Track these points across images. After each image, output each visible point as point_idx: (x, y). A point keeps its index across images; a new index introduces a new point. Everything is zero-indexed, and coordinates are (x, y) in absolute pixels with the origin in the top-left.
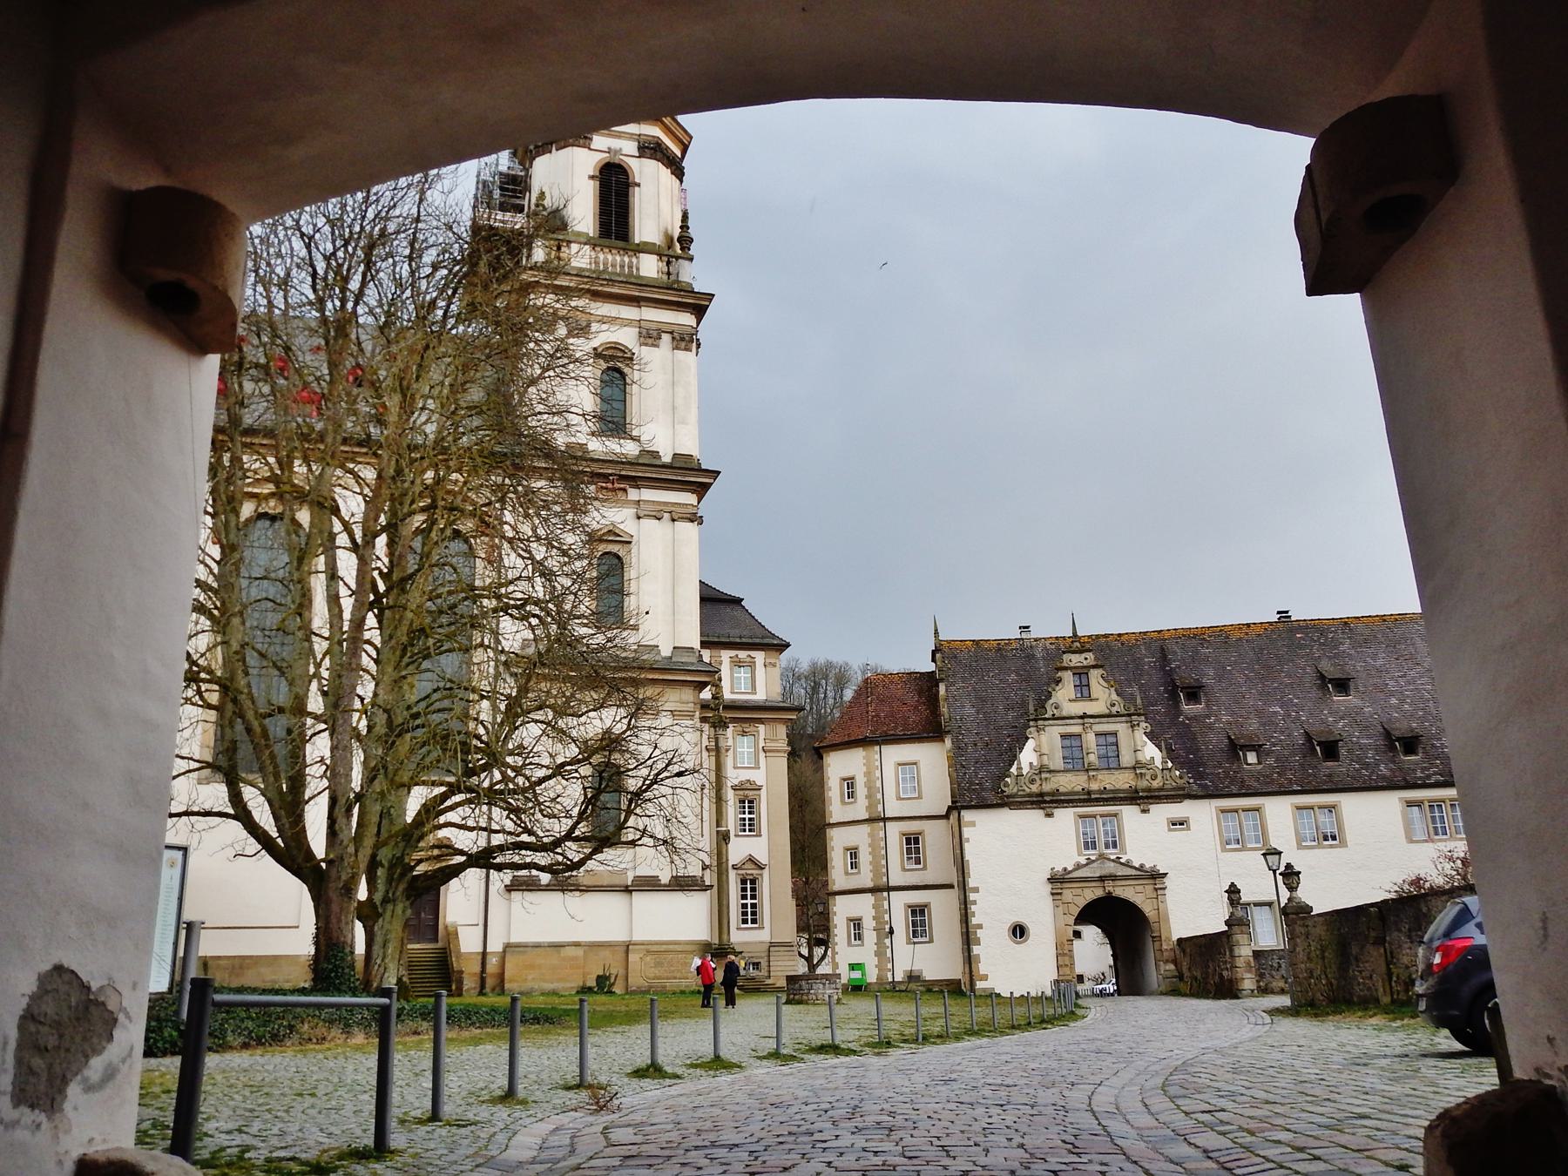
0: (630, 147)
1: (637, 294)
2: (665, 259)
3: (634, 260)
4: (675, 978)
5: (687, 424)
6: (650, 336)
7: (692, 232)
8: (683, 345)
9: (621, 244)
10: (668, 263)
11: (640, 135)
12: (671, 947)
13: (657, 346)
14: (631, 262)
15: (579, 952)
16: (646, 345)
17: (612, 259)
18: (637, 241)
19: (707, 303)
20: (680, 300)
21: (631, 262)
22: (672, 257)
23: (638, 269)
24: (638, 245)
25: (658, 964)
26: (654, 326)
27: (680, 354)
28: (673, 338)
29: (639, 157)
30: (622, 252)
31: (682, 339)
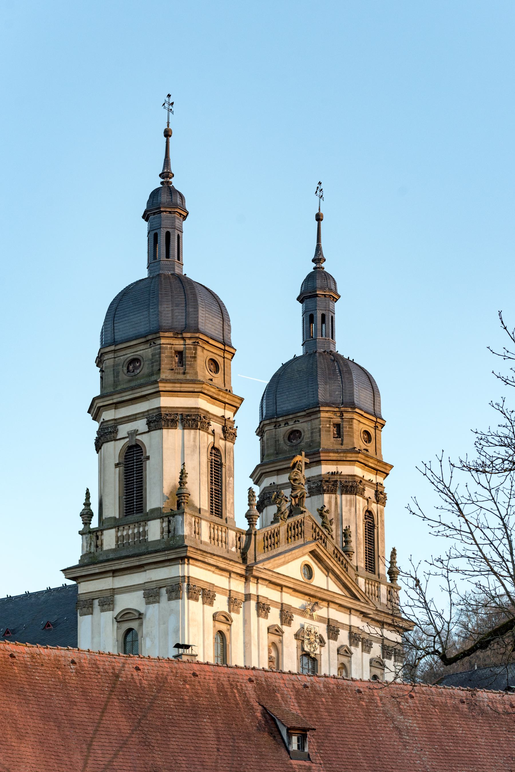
0: (141, 425)
2: (166, 519)
8: (174, 594)
11: (148, 411)
22: (171, 516)
26: (153, 585)
27: (173, 603)
29: (148, 432)
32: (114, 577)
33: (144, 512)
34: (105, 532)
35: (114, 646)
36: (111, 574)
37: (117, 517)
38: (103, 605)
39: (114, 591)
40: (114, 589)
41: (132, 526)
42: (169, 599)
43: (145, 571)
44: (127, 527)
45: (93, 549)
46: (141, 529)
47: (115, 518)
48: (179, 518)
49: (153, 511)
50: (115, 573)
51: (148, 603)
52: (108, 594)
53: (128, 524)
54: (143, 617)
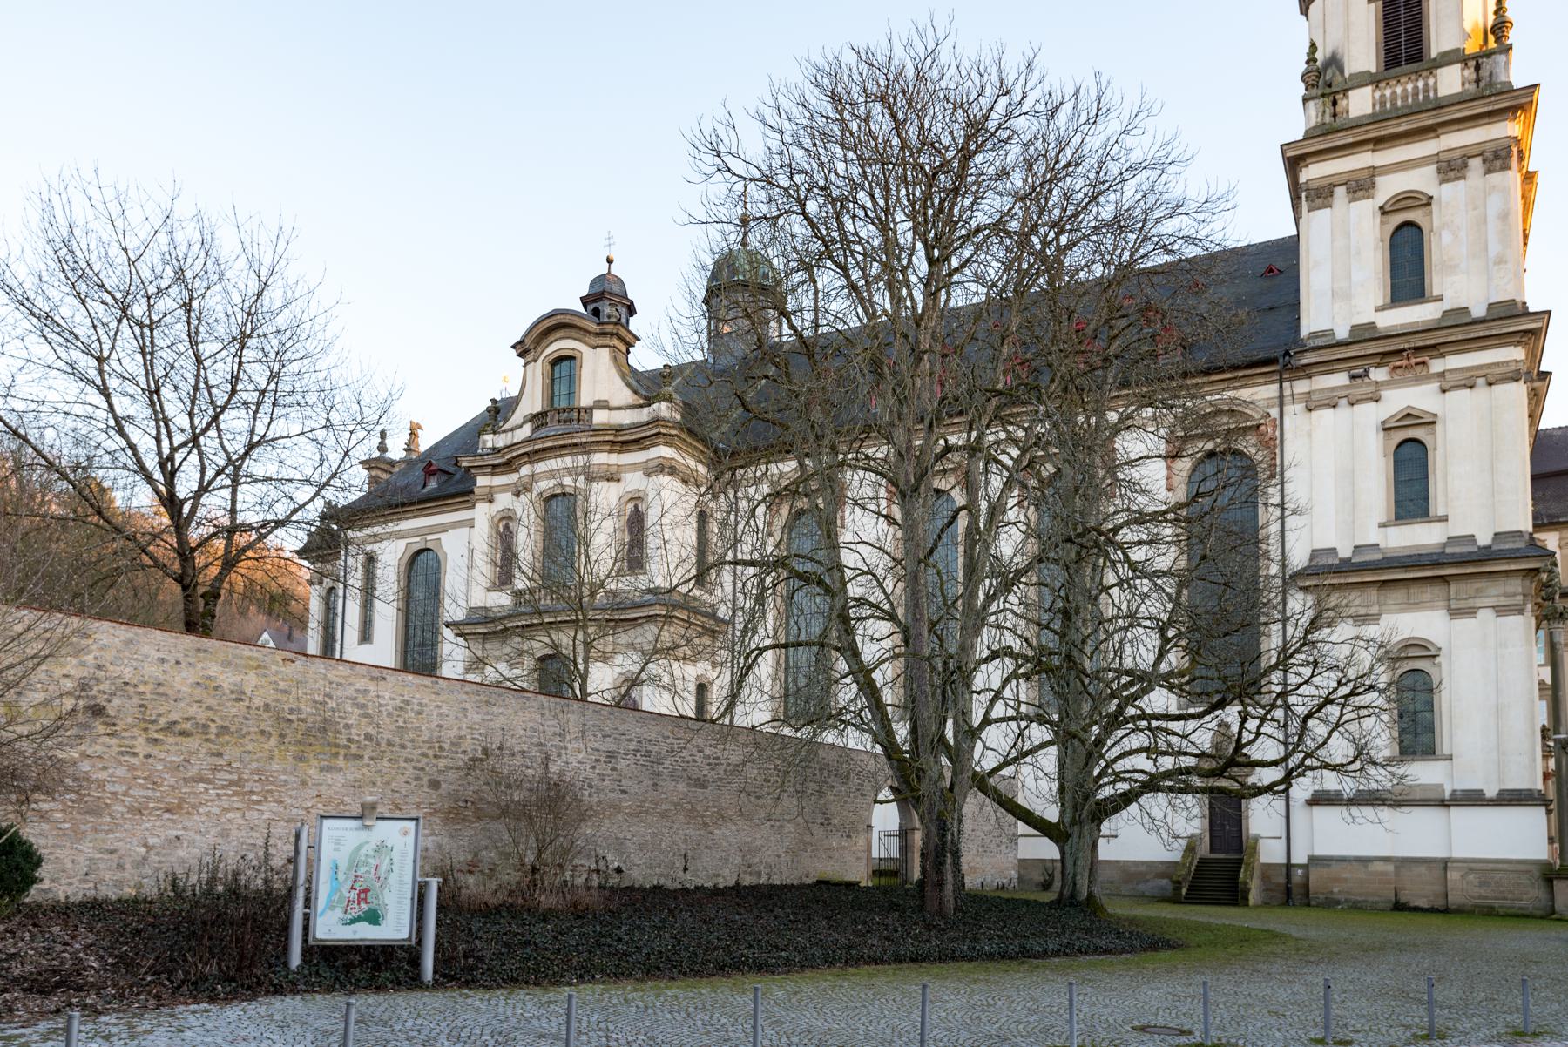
1: (1431, 122)
3: (1431, 81)
4: (1505, 899)
5: (1506, 262)
6: (1452, 168)
7: (1510, 15)
8: (1498, 163)
9: (1415, 66)
10: (1478, 68)
12: (1500, 866)
13: (1464, 178)
14: (1426, 85)
15: (1390, 868)
16: (1448, 181)
17: (1403, 89)
18: (1434, 54)
19: (1529, 99)
20: (1490, 108)
21: (1426, 85)
22: (1481, 57)
23: (1436, 90)
24: (1435, 59)
25: (1483, 884)
26: (1457, 154)
27: (1496, 178)
28: (1484, 161)
30: (1413, 77)
31: (1497, 157)
32: (1373, 151)
33: (1426, 59)
34: (1351, 93)
35: (1375, 249)
36: (1371, 147)
37: (1374, 70)
38: (1355, 192)
39: (1373, 172)
40: (1374, 168)
41: (1403, 80)
42: (1489, 171)
43: (1438, 137)
44: (1393, 82)
45: (1328, 119)
46: (1421, 84)
47: (1369, 72)
48: (1502, 58)
49: (1444, 55)
50: (1378, 143)
51: (1442, 182)
52: (1365, 174)
53: (1397, 78)
54: (1433, 202)
